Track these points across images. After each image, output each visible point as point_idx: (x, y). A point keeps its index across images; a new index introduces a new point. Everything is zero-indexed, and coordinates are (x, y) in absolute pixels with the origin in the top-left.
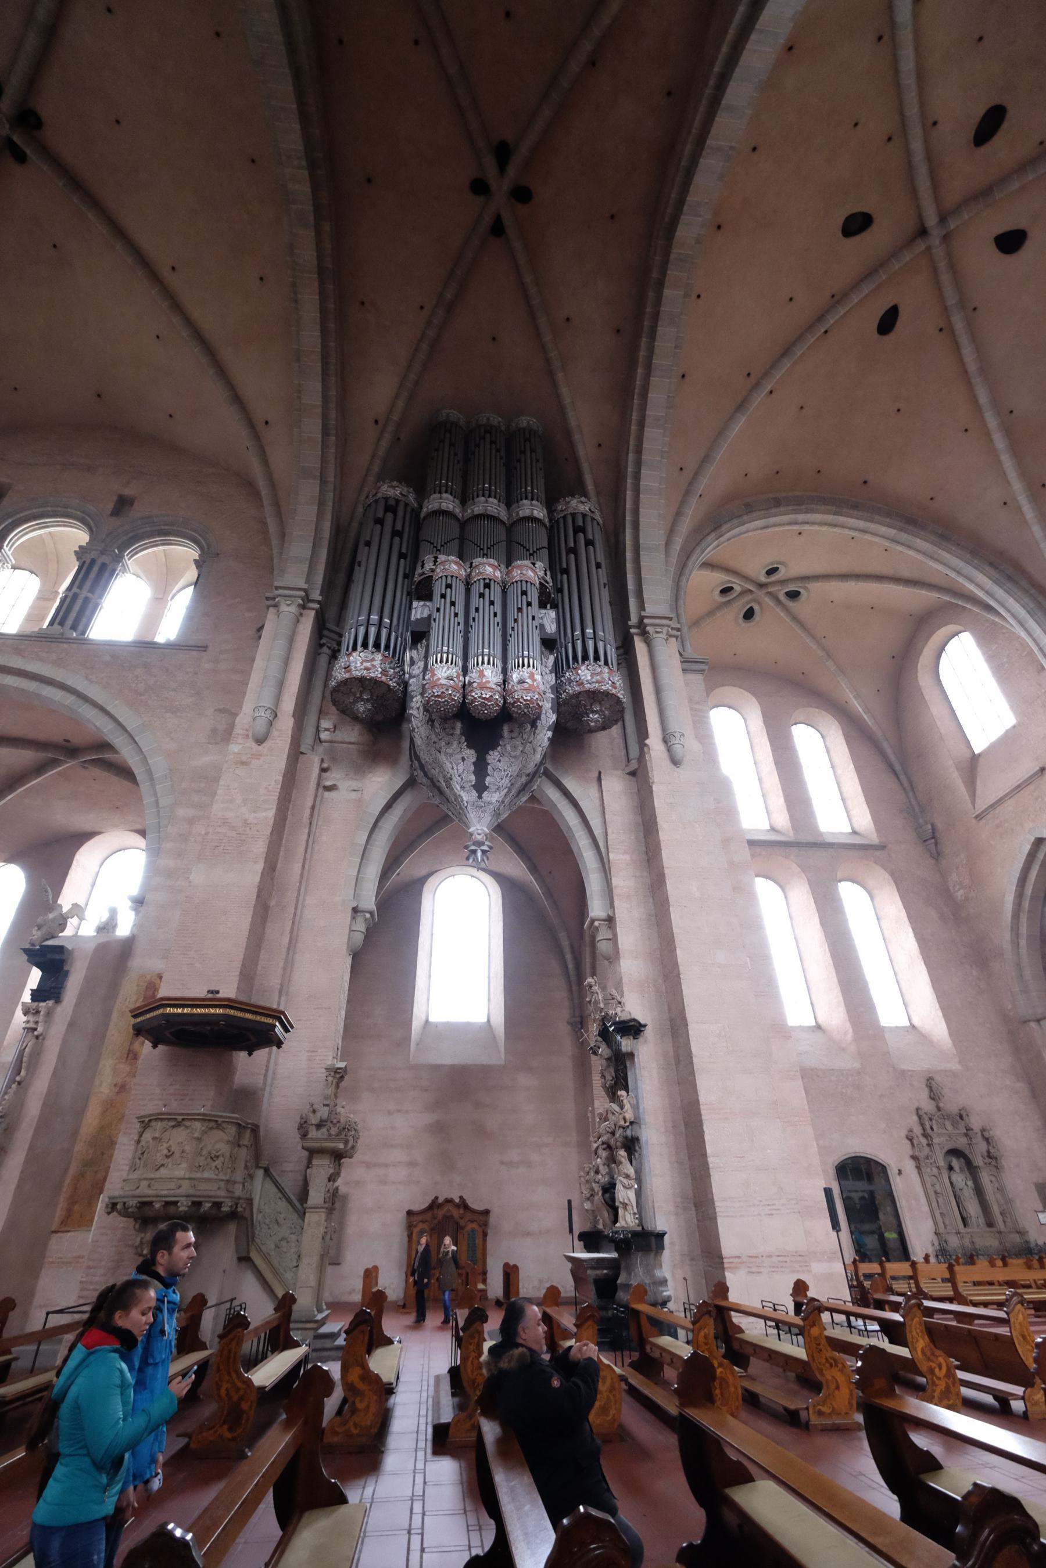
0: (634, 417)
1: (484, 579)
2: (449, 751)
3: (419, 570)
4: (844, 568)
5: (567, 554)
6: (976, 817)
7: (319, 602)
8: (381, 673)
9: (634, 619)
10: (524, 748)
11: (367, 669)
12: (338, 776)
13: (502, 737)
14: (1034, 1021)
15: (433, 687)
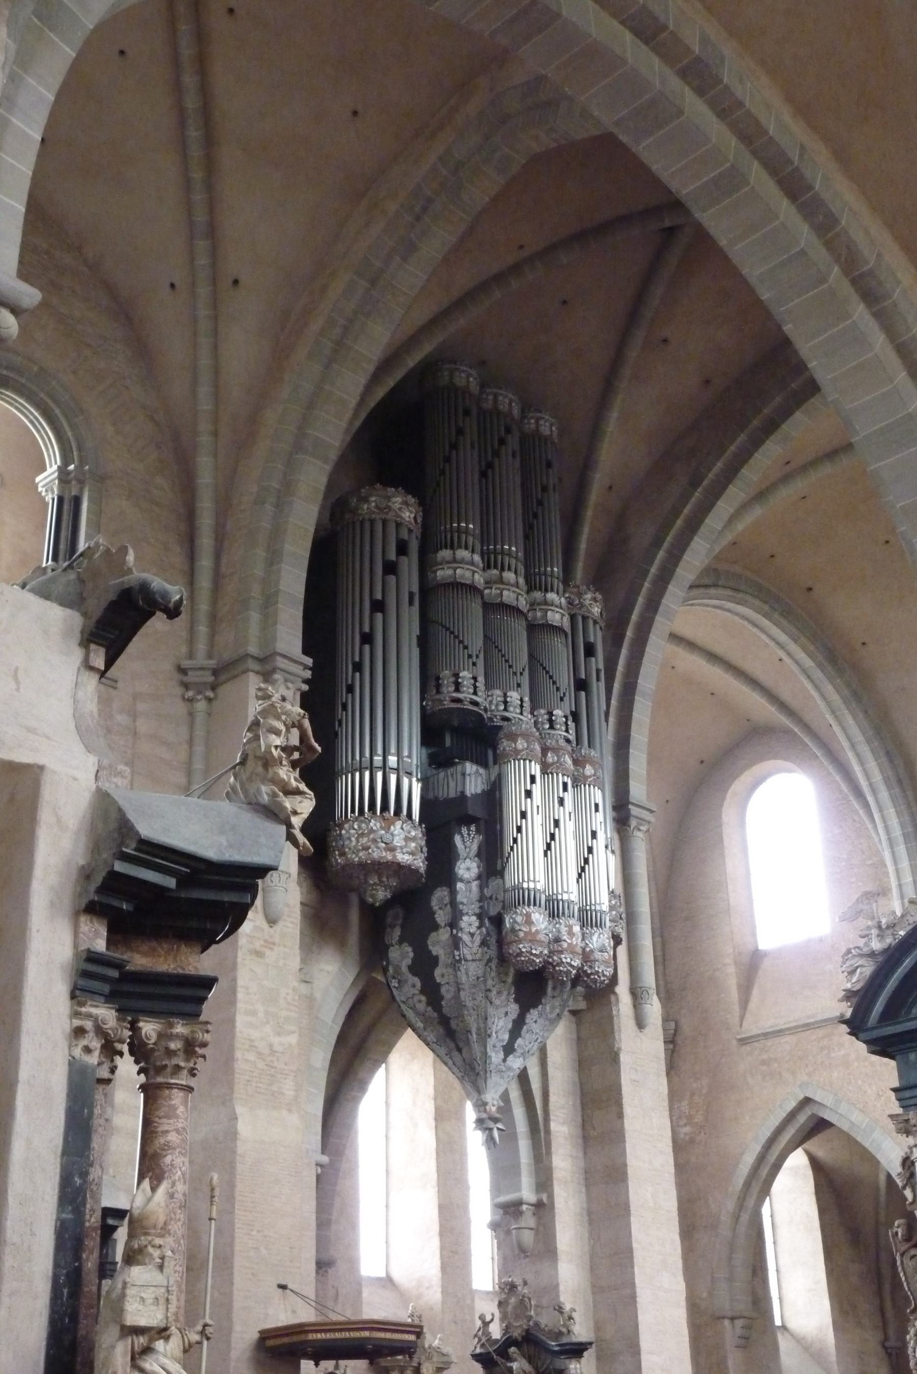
0: (686, 511)
4: (718, 649)
6: (741, 1040)
13: (544, 993)
14: (728, 1318)
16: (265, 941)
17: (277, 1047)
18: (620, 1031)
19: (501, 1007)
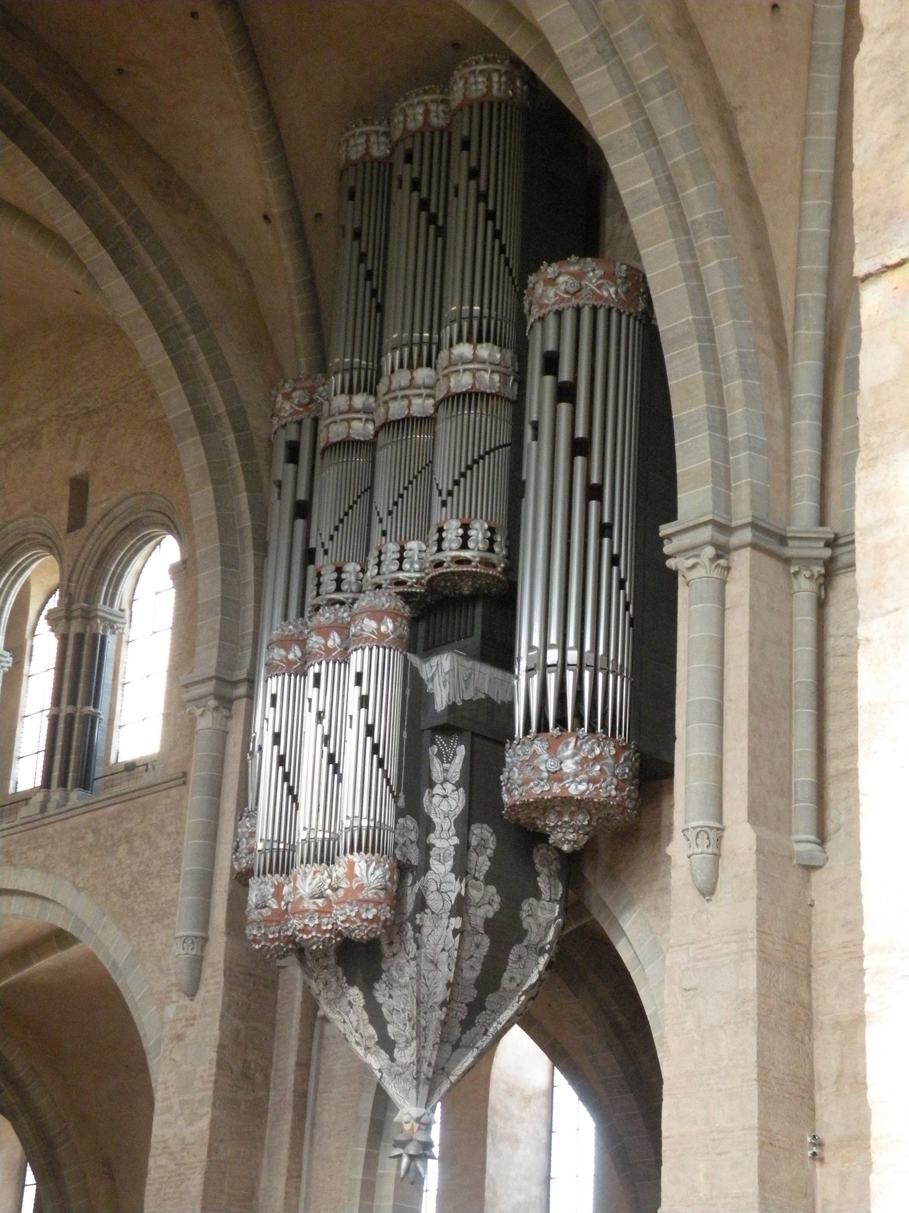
2: (331, 995)
16: (187, 1020)
17: (189, 1140)
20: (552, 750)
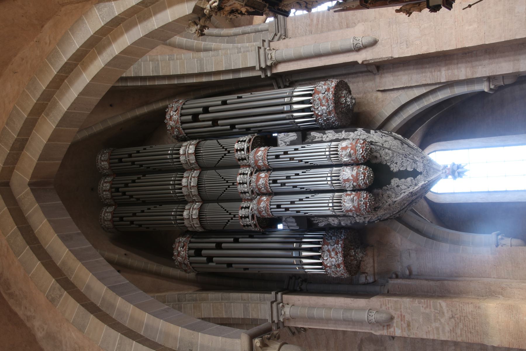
1: (269, 184)
3: (253, 228)
5: (218, 125)
7: (277, 293)
8: (338, 244)
9: (259, 73)
10: (386, 148)
11: (336, 254)
12: (400, 267)
15: (360, 210)
16: (402, 321)
18: (382, 58)
19: (395, 192)
20: (319, 93)
